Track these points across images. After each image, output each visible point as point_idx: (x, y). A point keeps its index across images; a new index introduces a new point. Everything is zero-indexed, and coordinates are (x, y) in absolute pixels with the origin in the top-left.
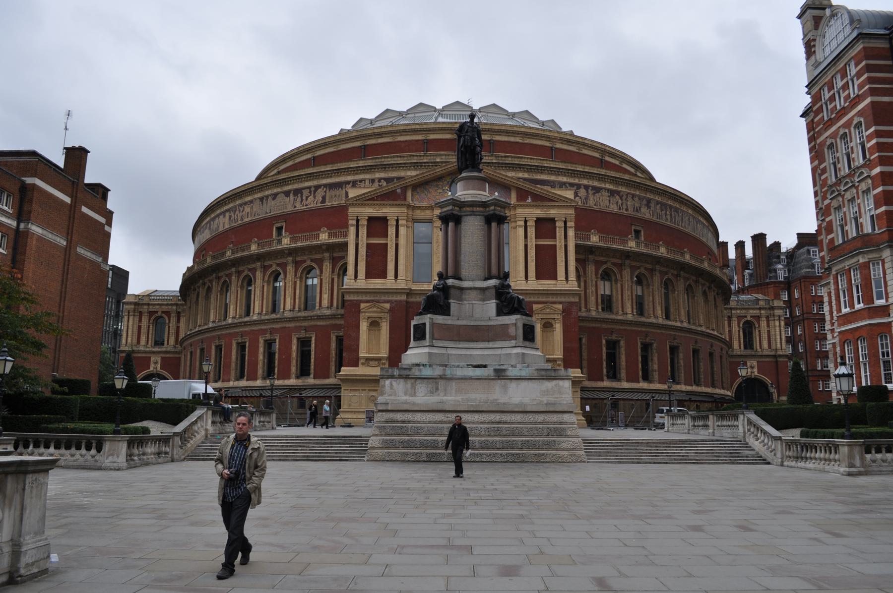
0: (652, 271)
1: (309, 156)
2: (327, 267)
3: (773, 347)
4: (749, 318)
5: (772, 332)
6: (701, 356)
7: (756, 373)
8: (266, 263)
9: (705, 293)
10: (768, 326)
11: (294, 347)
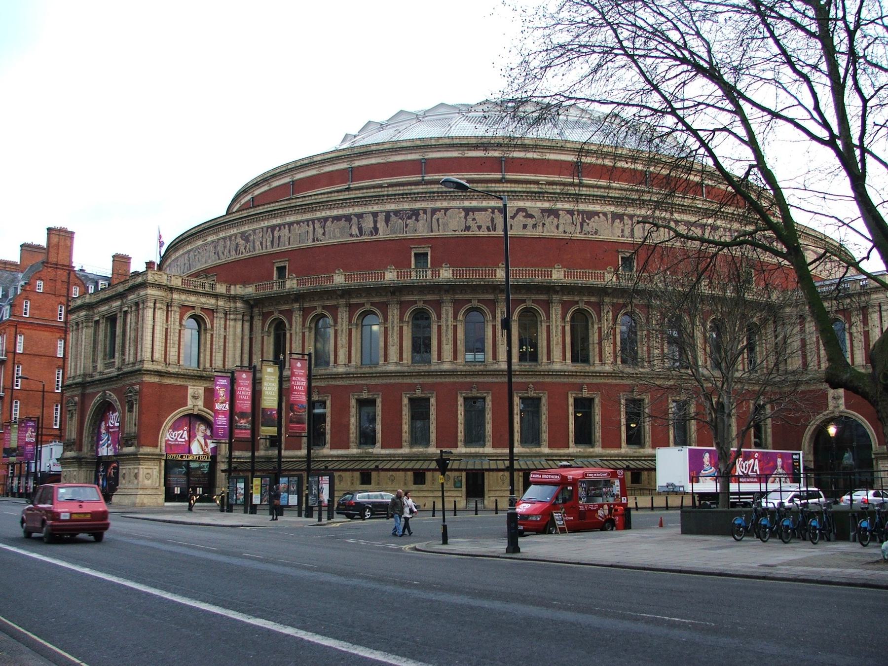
7: (842, 408)
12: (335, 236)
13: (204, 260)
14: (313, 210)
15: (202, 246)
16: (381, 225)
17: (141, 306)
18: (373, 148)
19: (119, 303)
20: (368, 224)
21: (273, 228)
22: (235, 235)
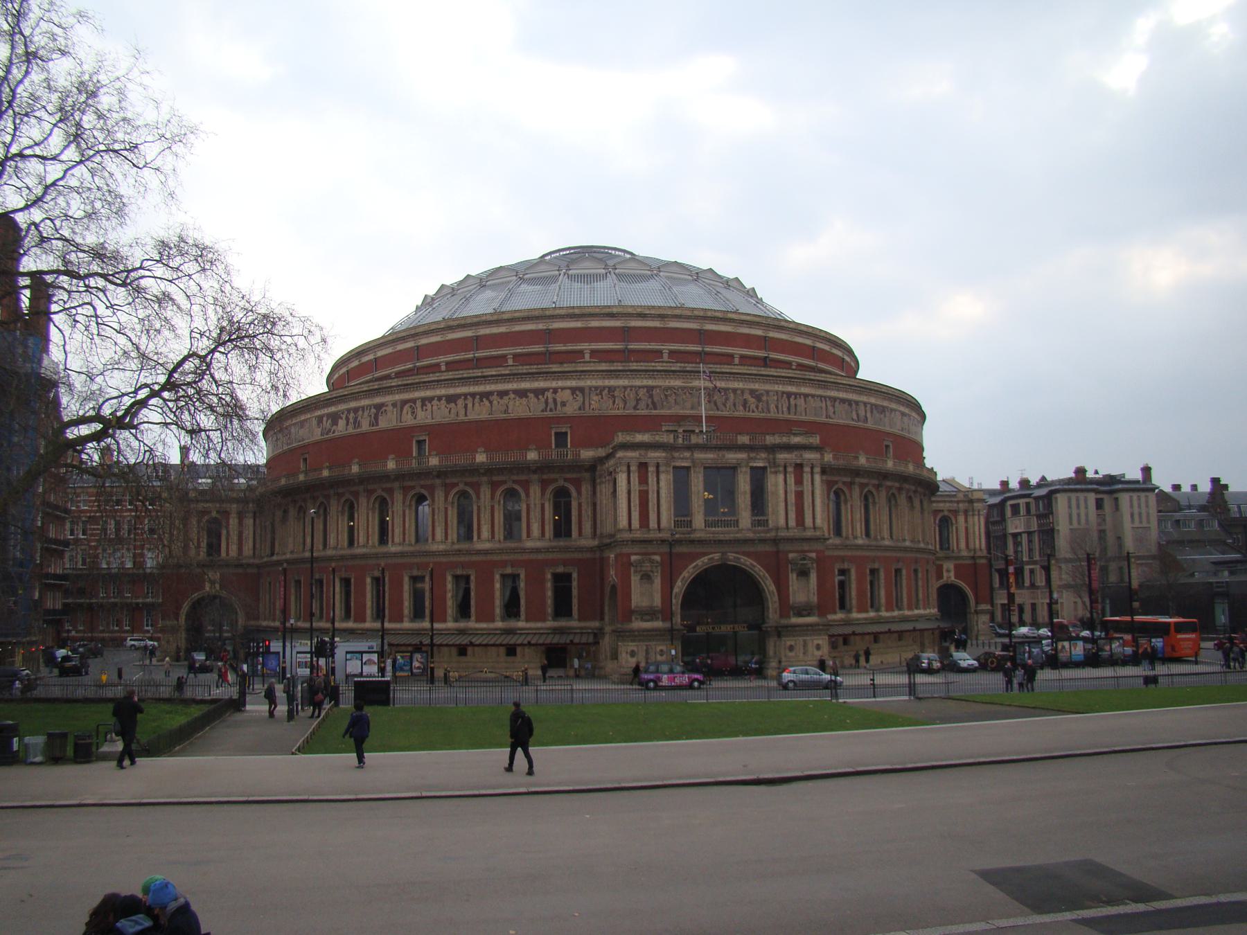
0: (878, 487)
1: (468, 333)
2: (535, 490)
3: (971, 546)
4: (946, 513)
5: (971, 531)
6: (920, 575)
8: (448, 481)
9: (921, 502)
10: (966, 521)
11: (498, 586)
12: (841, 417)
13: (688, 405)
14: (826, 388)
15: (683, 388)
16: (869, 415)
17: (807, 469)
18: (783, 324)
19: (743, 455)
20: (862, 413)
21: (789, 395)
22: (743, 391)
